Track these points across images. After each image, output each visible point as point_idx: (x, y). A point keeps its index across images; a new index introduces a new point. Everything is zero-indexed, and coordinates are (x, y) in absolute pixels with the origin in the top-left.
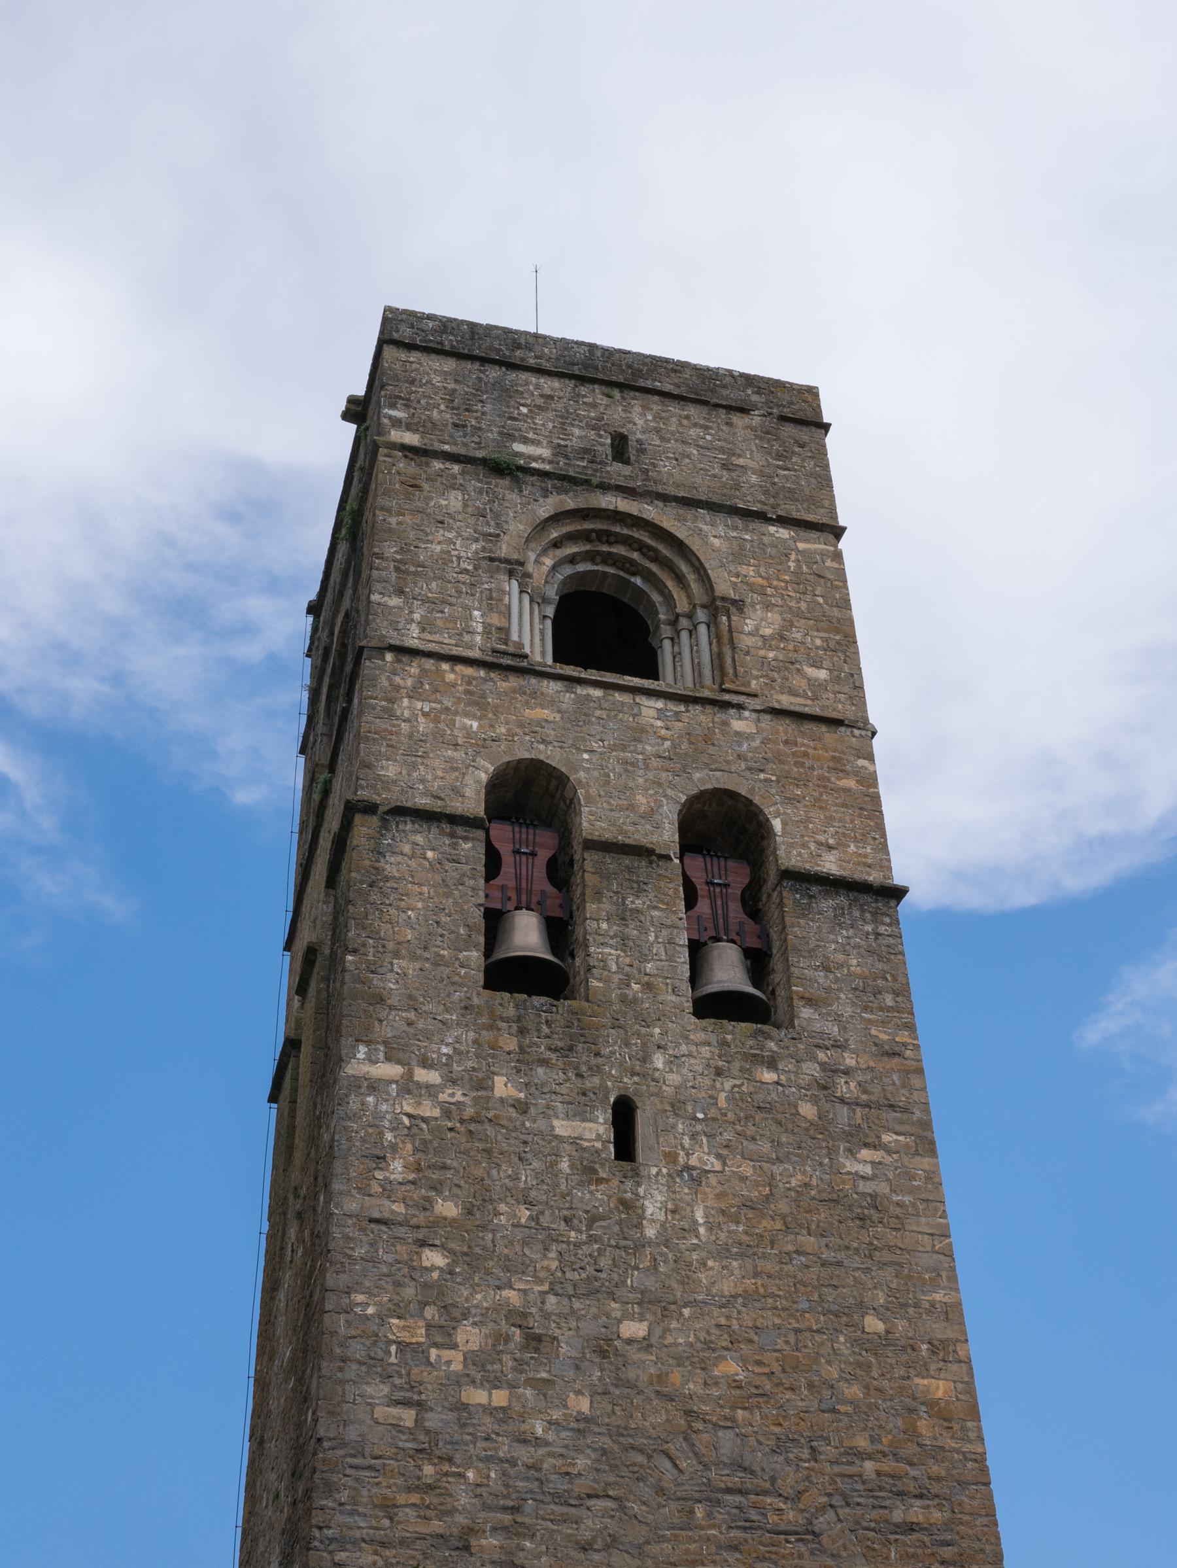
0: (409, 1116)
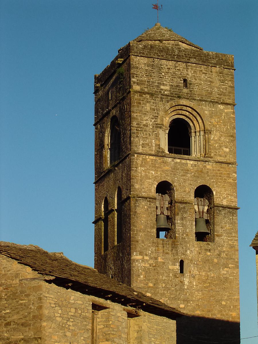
0: (144, 266)
